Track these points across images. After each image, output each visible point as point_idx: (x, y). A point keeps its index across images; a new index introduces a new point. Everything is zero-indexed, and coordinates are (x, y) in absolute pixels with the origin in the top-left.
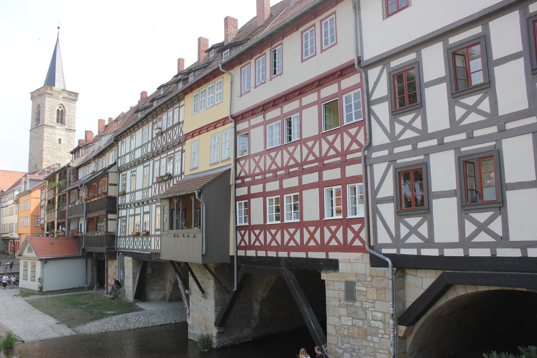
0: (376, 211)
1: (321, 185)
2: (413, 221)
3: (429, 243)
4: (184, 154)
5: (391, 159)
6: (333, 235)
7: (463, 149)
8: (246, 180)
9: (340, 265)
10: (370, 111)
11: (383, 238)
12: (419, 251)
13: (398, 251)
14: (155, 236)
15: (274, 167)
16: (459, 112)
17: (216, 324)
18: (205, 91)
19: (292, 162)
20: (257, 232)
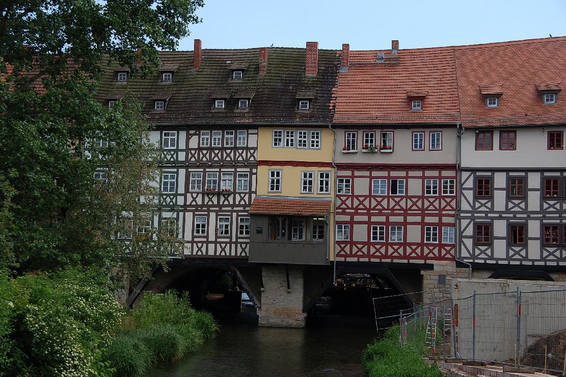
0: (461, 242)
1: (423, 224)
2: (483, 248)
3: (491, 258)
4: (254, 177)
5: (472, 218)
6: (431, 251)
7: (510, 221)
8: (347, 211)
9: (434, 267)
10: (462, 192)
11: (464, 253)
12: (485, 261)
13: (474, 261)
14: (192, 242)
15: (379, 207)
16: (511, 205)
17: (304, 311)
18: (292, 133)
19: (398, 207)
20: (360, 246)
